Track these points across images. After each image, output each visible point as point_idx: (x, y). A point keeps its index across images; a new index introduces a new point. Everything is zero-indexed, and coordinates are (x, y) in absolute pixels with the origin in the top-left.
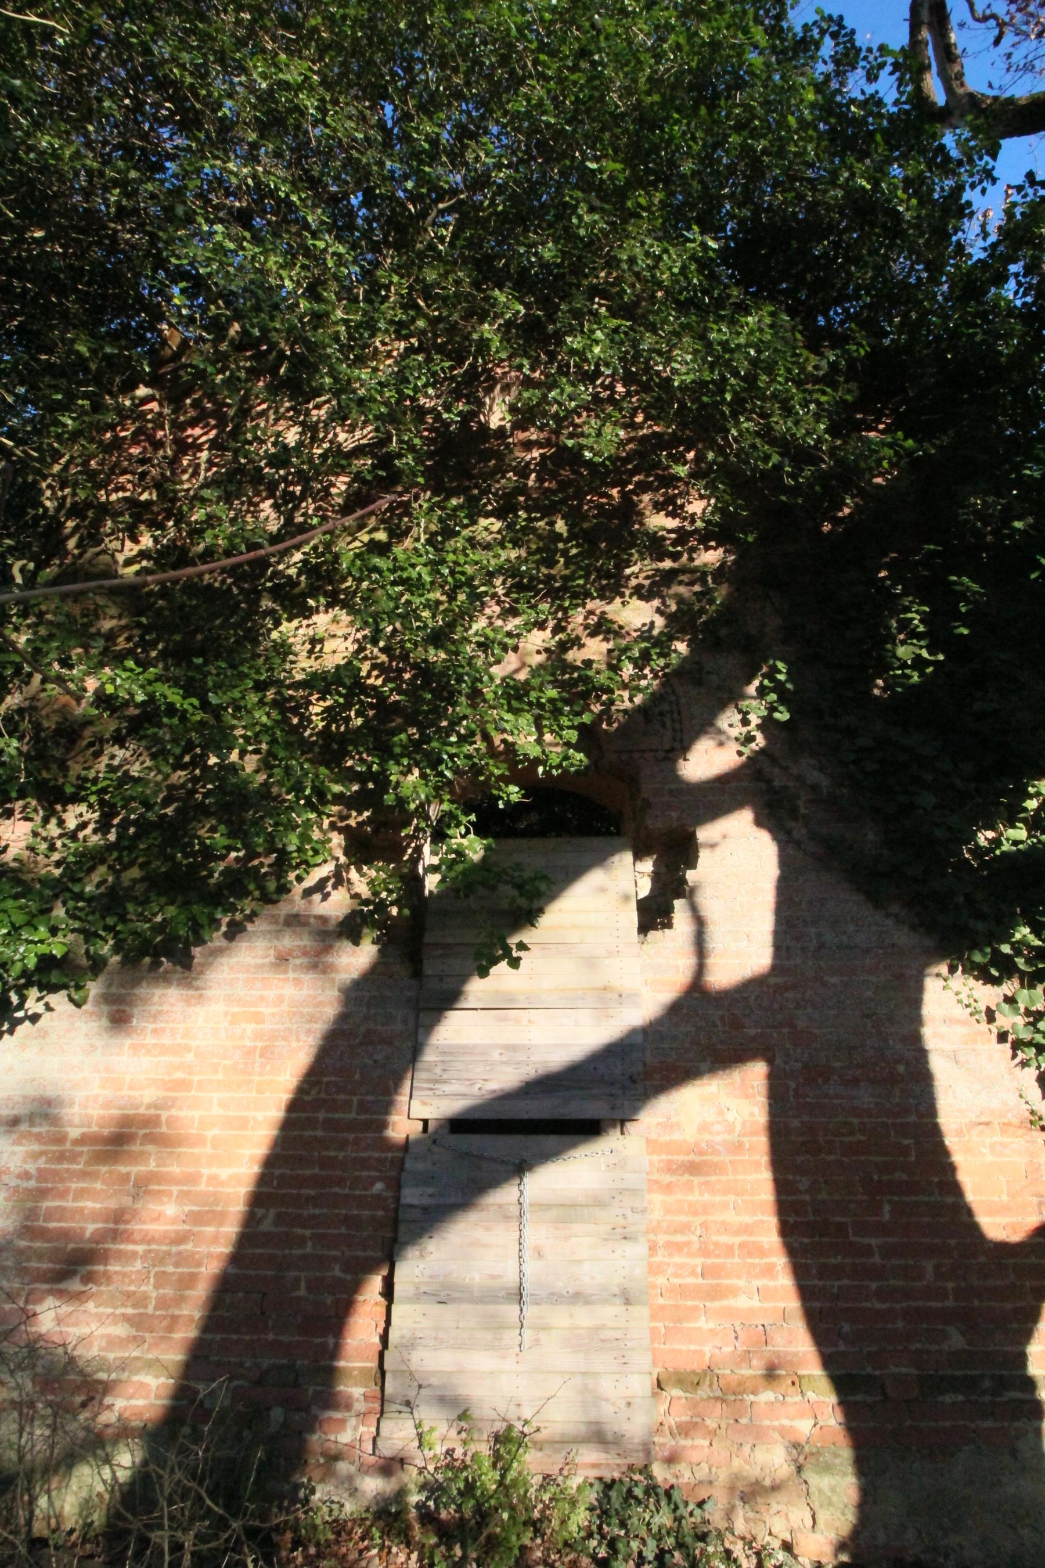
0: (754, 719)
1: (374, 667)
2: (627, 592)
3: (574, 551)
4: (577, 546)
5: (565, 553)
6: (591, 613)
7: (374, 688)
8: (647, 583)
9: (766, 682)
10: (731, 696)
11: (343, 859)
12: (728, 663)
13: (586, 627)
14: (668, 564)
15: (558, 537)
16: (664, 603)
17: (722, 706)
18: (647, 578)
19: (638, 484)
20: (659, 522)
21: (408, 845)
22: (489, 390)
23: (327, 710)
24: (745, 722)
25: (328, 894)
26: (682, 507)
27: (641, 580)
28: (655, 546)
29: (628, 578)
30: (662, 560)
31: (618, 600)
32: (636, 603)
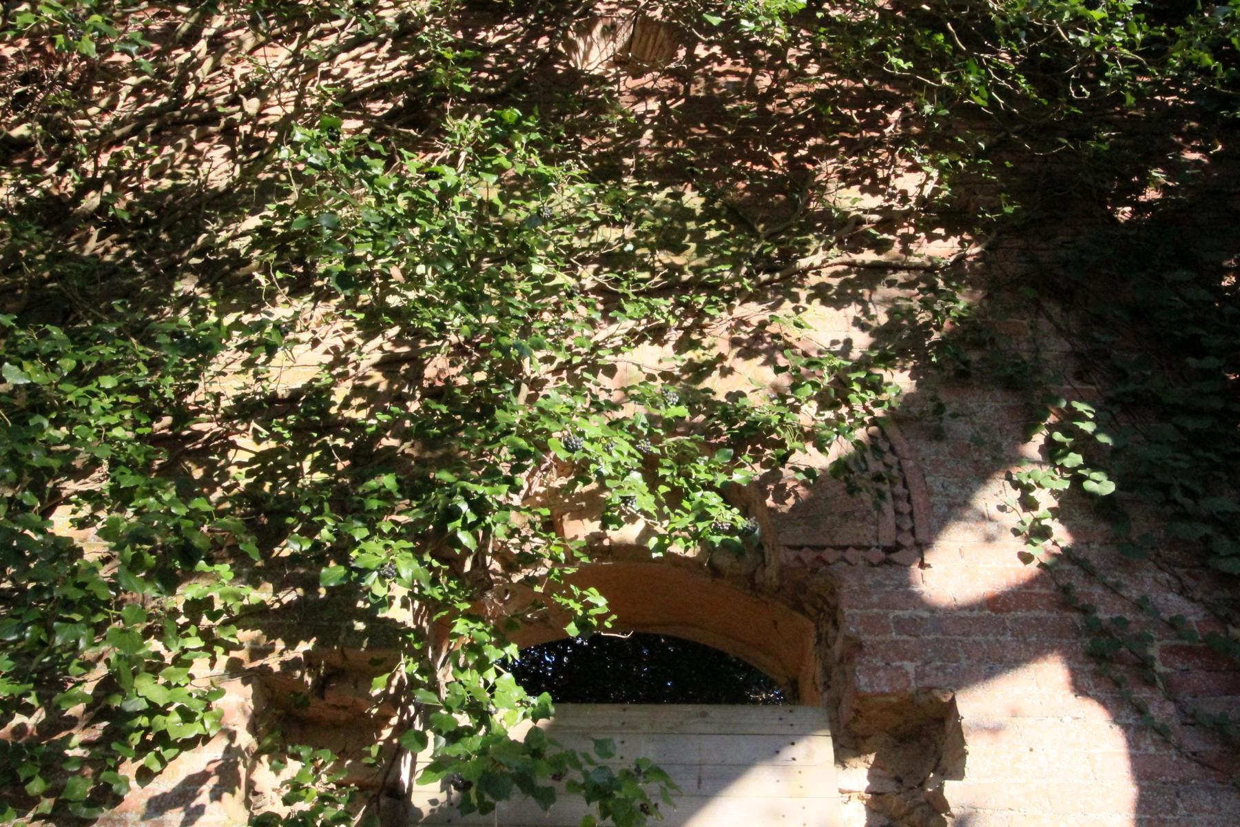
0: (1045, 500)
1: (357, 390)
2: (803, 294)
3: (713, 234)
4: (719, 226)
5: (698, 236)
6: (742, 322)
7: (352, 423)
8: (835, 282)
9: (1058, 436)
10: (993, 459)
11: (245, 739)
12: (988, 406)
13: (735, 342)
14: (868, 256)
15: (689, 214)
16: (866, 312)
17: (984, 477)
18: (835, 275)
19: (813, 150)
20: (851, 200)
21: (383, 720)
22: (585, 30)
23: (261, 457)
24: (1028, 504)
25: (200, 810)
26: (886, 180)
27: (824, 278)
28: (847, 231)
29: (804, 273)
30: (857, 251)
31: (788, 305)
32: (817, 312)
